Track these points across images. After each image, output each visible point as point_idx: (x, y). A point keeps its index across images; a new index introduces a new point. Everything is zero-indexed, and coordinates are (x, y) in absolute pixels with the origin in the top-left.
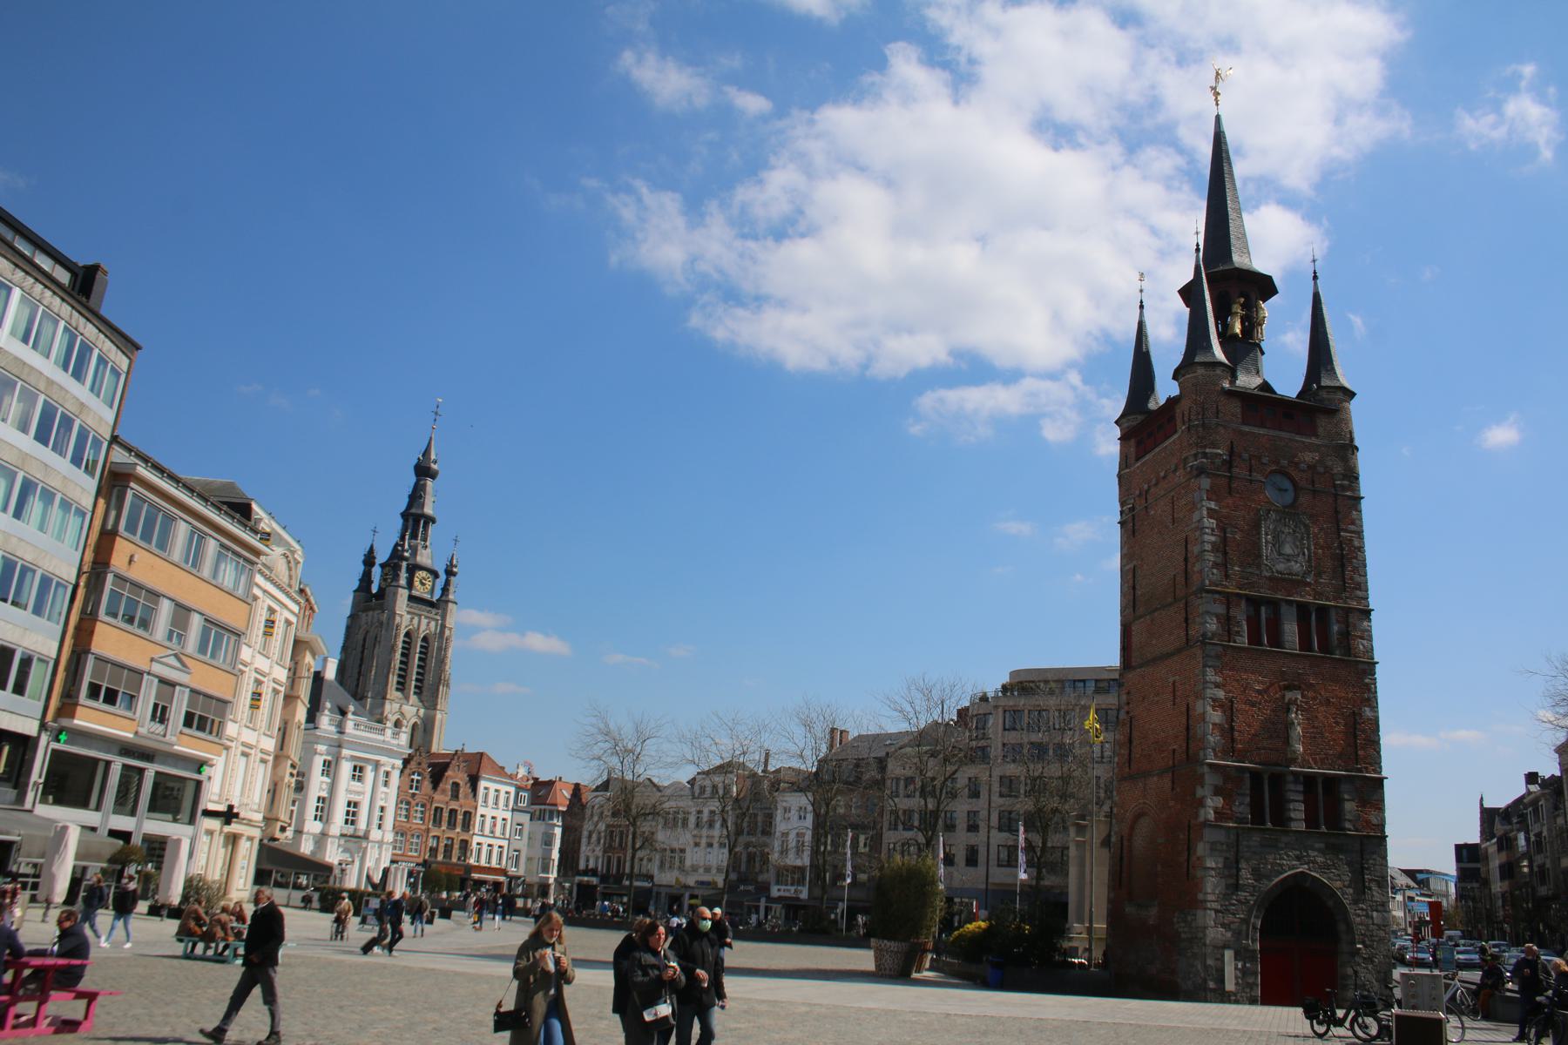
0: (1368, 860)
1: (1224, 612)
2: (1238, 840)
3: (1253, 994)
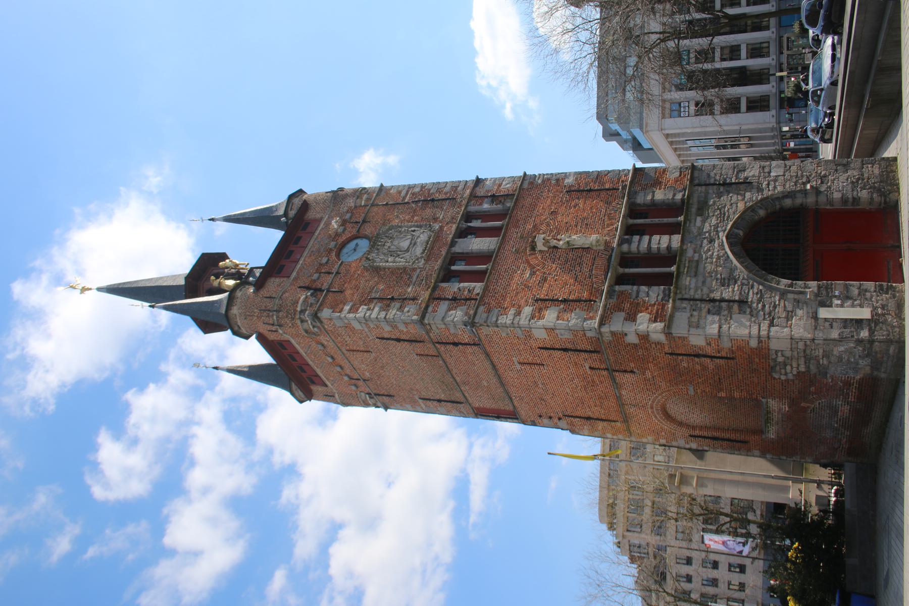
0: (715, 180)
1: (447, 302)
2: (690, 300)
3: (872, 289)
